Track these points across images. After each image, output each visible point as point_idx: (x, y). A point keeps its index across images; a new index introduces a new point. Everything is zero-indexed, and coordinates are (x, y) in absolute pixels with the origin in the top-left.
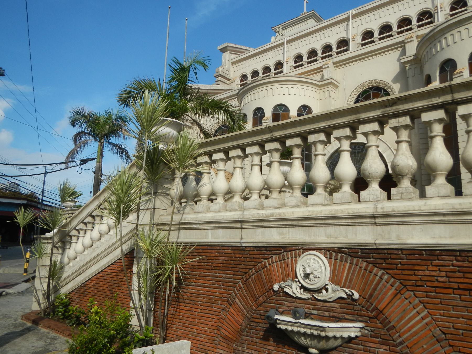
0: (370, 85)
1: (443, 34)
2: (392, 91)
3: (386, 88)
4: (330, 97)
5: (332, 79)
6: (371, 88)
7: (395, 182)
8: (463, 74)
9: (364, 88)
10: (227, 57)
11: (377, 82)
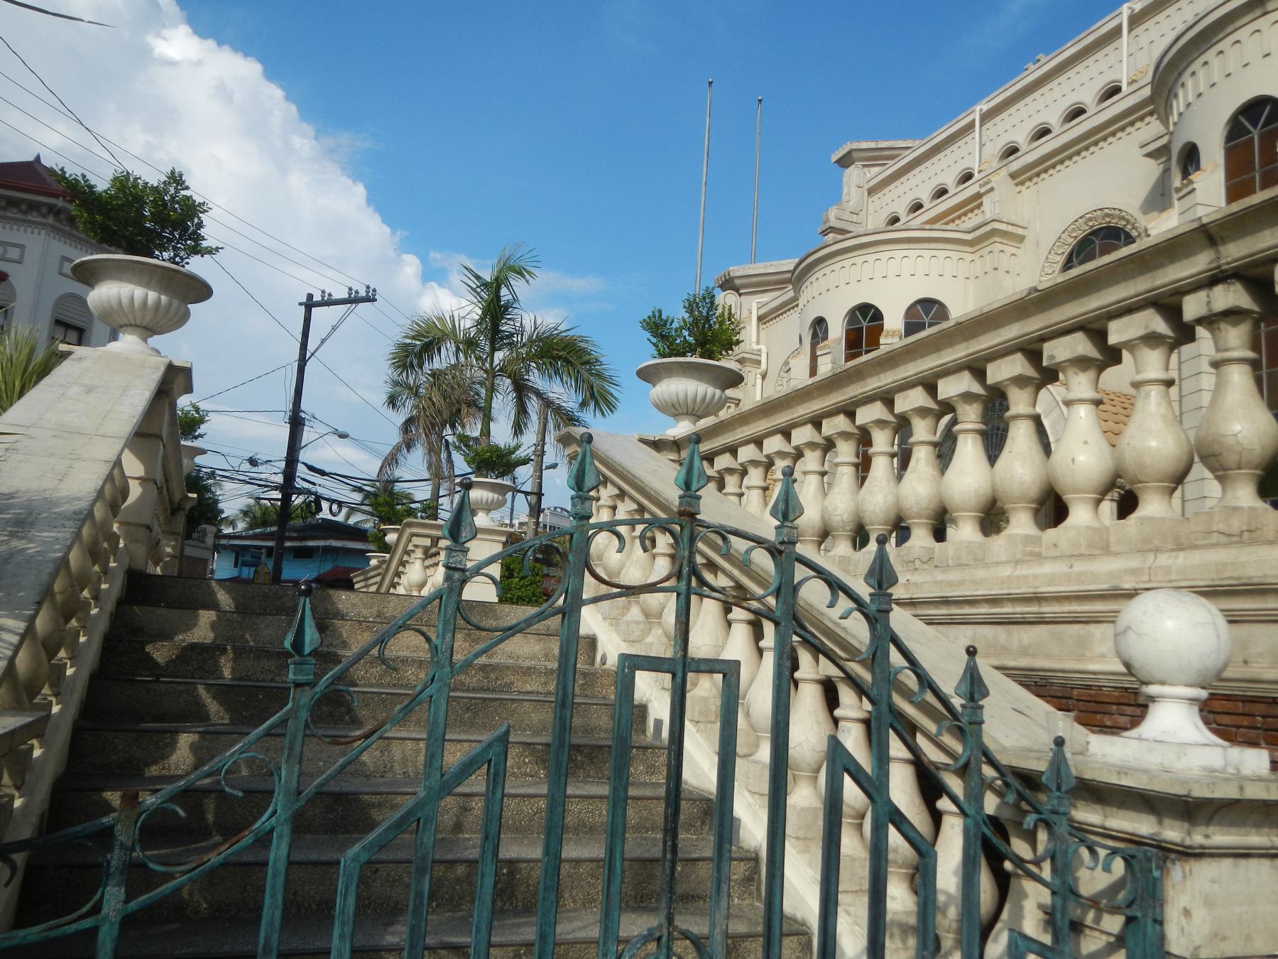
0: (1091, 224)
1: (1176, 74)
5: (994, 220)
6: (1095, 233)
8: (1195, 186)
10: (855, 177)
11: (1108, 215)
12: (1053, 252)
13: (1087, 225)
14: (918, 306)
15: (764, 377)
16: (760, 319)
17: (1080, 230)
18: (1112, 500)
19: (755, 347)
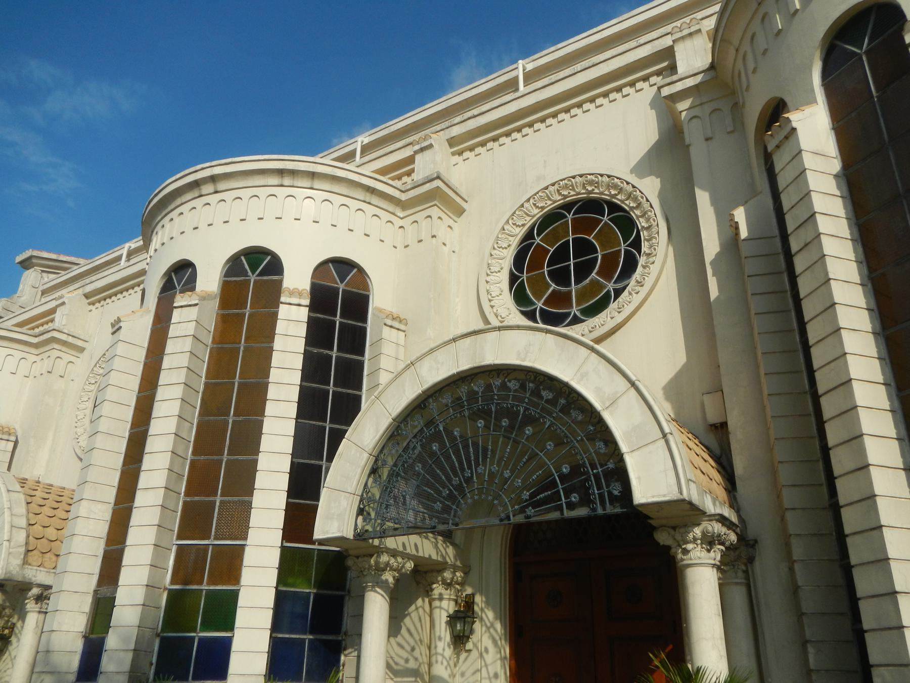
0: (565, 193)
2: (639, 205)
3: (619, 199)
4: (434, 236)
6: (568, 207)
7: (668, 548)
9: (549, 206)
11: (591, 183)
12: (510, 222)
13: (560, 194)
14: (330, 265)
17: (550, 199)
18: (714, 565)
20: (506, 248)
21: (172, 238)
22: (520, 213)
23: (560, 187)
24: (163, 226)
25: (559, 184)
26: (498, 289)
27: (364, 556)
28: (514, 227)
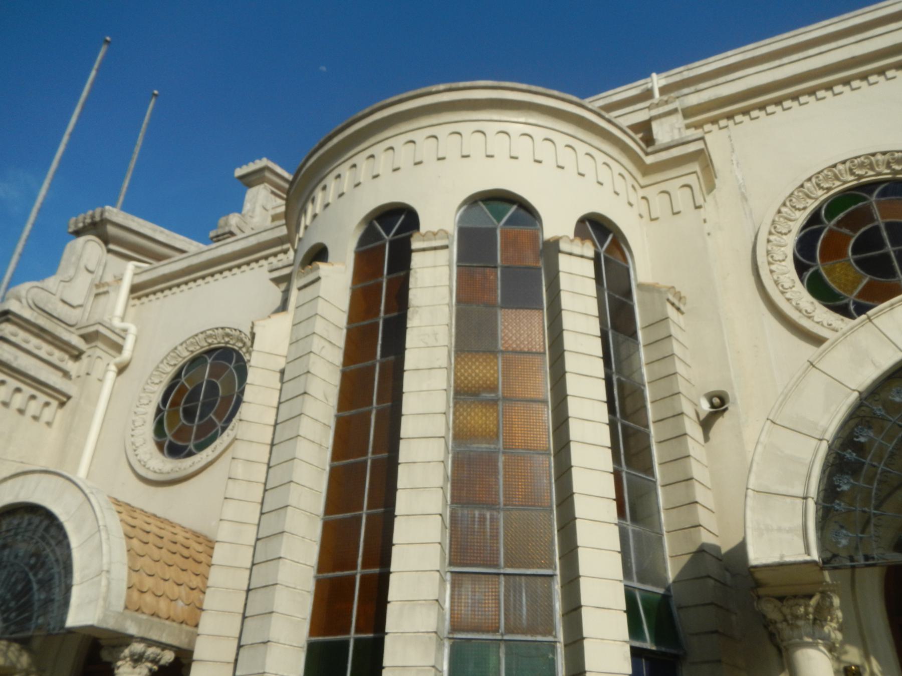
6: (869, 187)
9: (837, 187)
12: (788, 203)
15: (122, 369)
16: (135, 289)
19: (117, 323)
20: (786, 234)
21: (341, 195)
22: (800, 194)
23: (854, 166)
24: (339, 176)
25: (852, 162)
26: (788, 280)
27: (795, 597)
28: (793, 210)
